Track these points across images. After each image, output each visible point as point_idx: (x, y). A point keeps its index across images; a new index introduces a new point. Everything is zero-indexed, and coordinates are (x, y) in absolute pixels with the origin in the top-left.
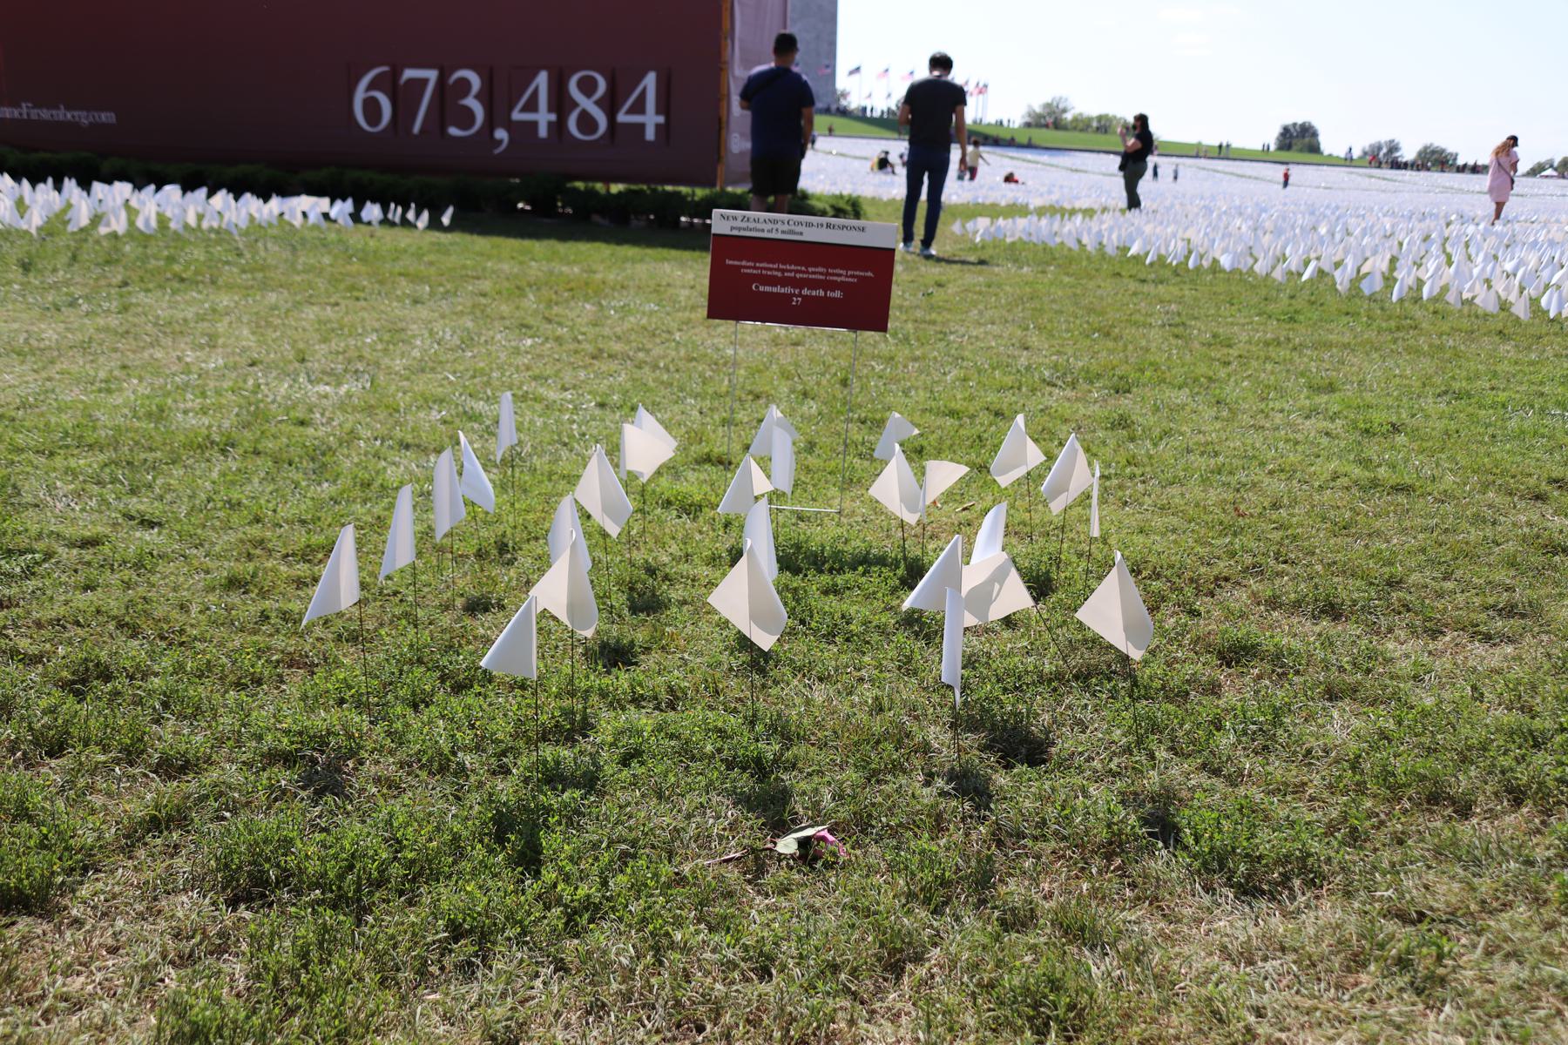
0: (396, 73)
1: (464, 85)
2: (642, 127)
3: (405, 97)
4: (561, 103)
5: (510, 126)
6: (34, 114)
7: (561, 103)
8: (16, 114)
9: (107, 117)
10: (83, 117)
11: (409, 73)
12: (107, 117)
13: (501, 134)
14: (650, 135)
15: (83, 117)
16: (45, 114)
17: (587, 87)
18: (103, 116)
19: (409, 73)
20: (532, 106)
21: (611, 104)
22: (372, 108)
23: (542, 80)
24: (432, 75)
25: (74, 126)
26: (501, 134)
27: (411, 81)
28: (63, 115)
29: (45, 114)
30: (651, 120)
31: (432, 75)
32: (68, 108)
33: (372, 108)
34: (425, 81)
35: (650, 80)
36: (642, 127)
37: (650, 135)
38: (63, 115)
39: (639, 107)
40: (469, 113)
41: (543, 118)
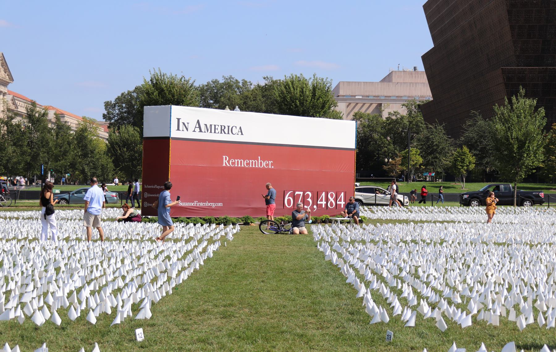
1: (308, 195)
2: (341, 204)
3: (295, 198)
4: (327, 200)
5: (317, 205)
7: (327, 200)
9: (220, 204)
10: (213, 205)
11: (297, 193)
12: (220, 204)
15: (213, 205)
16: (201, 204)
17: (332, 197)
19: (297, 193)
20: (321, 200)
21: (336, 200)
23: (324, 194)
24: (301, 193)
27: (297, 194)
28: (207, 204)
29: (201, 204)
30: (343, 203)
31: (301, 193)
33: (289, 201)
35: (342, 194)
36: (341, 204)
37: (342, 207)
38: (207, 204)
39: (340, 201)
40: (309, 202)
41: (324, 203)
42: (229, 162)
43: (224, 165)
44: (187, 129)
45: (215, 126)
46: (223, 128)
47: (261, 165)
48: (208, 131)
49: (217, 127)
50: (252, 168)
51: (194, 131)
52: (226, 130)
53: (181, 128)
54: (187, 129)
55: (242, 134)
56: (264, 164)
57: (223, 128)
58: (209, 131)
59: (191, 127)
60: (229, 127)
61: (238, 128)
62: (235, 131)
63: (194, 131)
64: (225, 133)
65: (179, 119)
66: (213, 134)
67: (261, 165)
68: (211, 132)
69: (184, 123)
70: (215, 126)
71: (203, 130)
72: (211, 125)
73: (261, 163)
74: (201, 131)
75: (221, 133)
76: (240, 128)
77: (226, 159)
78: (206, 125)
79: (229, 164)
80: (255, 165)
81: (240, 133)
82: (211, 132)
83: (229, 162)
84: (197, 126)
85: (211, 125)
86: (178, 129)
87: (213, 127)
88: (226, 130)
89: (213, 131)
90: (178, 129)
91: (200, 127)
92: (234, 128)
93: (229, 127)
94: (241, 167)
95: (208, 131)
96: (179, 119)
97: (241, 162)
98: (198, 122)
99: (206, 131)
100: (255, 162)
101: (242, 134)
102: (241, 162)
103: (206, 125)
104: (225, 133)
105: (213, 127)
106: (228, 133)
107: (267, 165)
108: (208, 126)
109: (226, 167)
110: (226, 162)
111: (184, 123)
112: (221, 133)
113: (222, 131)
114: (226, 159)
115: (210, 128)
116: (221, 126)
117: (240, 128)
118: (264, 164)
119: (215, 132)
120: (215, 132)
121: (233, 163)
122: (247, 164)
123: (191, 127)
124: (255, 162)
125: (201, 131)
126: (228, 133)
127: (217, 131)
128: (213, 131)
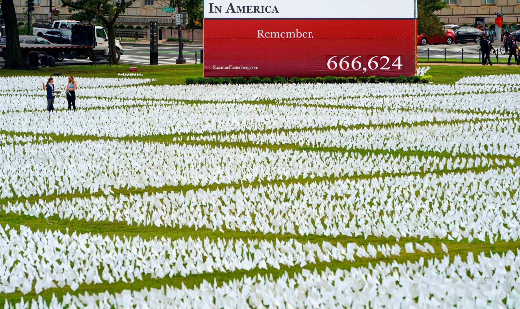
6: (233, 68)
8: (227, 68)
10: (248, 68)
13: (365, 69)
14: (399, 68)
15: (248, 68)
16: (236, 68)
18: (255, 68)
22: (332, 65)
26: (365, 69)
28: (242, 68)
29: (236, 68)
30: (399, 65)
33: (332, 65)
35: (399, 58)
37: (399, 68)
38: (242, 68)
39: (397, 63)
42: (264, 34)
43: (259, 37)
44: (220, 11)
45: (248, 7)
48: (241, 11)
50: (289, 39)
51: (227, 12)
52: (260, 10)
54: (220, 11)
55: (277, 12)
56: (303, 35)
57: (257, 8)
58: (242, 11)
59: (224, 9)
60: (263, 7)
61: (273, 8)
62: (269, 9)
63: (227, 12)
64: (259, 12)
65: (211, 5)
67: (299, 35)
68: (244, 12)
70: (248, 7)
72: (244, 7)
73: (299, 35)
74: (234, 11)
75: (255, 12)
78: (239, 7)
79: (264, 36)
82: (244, 12)
83: (264, 34)
84: (230, 8)
86: (211, 11)
88: (260, 10)
90: (211, 11)
91: (232, 9)
93: (263, 7)
94: (277, 38)
95: (241, 11)
96: (211, 5)
97: (277, 34)
98: (231, 5)
99: (239, 11)
100: (292, 34)
101: (277, 12)
102: (277, 34)
104: (259, 12)
106: (263, 12)
110: (260, 34)
111: (216, 7)
112: (255, 12)
113: (256, 10)
114: (261, 32)
115: (241, 9)
116: (255, 7)
117: (275, 7)
118: (303, 35)
119: (248, 12)
120: (248, 12)
122: (283, 36)
123: (224, 9)
124: (292, 34)
125: (234, 11)
126: (263, 12)
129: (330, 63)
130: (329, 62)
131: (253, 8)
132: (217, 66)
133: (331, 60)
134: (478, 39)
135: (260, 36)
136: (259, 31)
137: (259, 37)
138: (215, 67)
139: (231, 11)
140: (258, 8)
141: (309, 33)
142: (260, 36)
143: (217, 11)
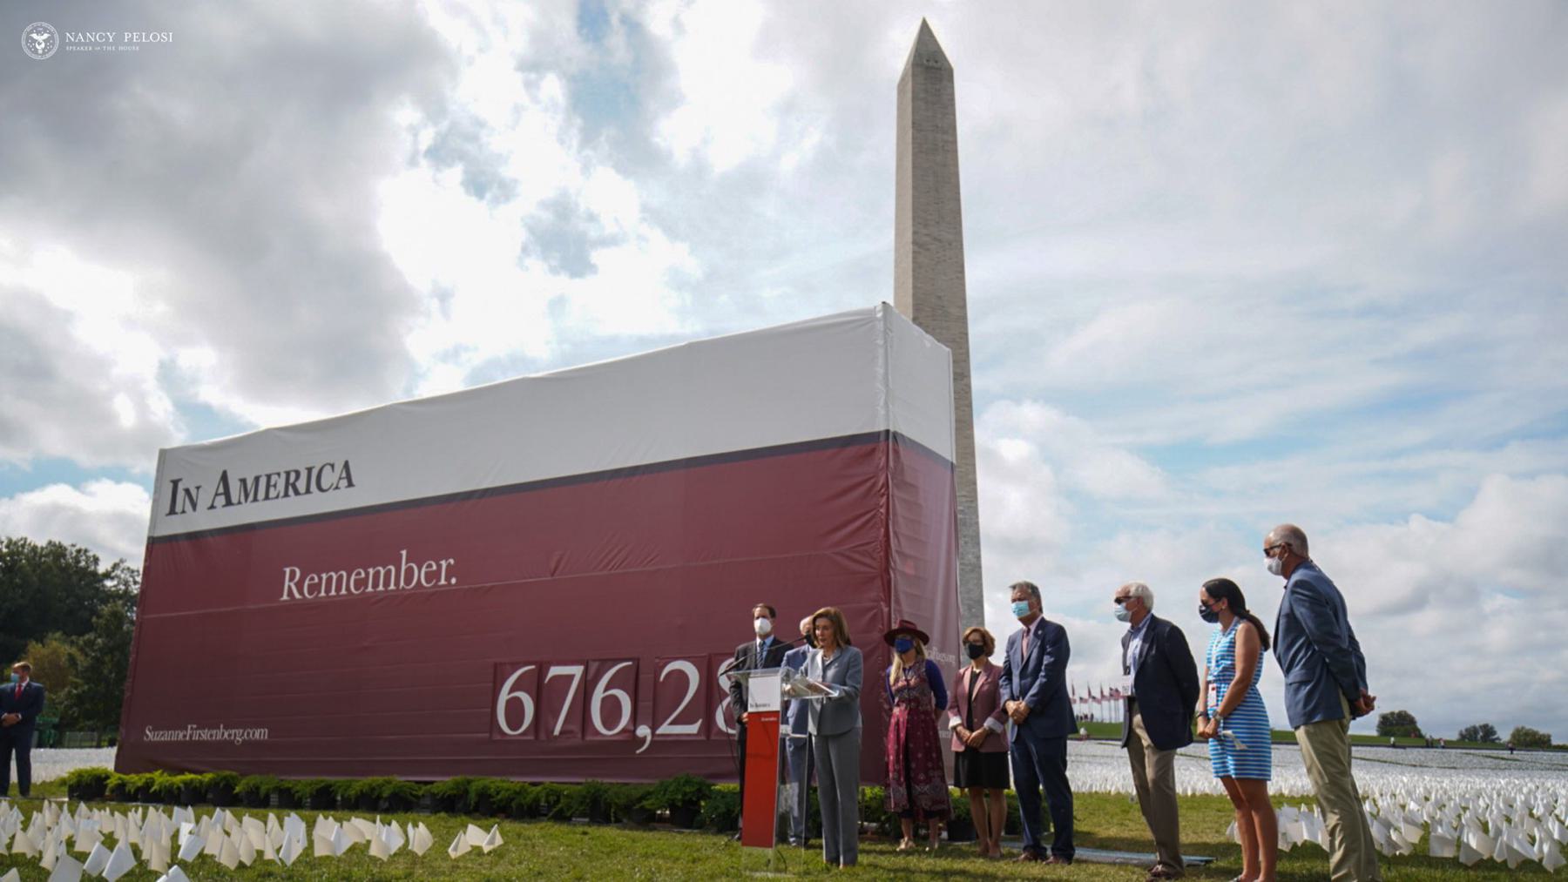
0: (542, 669)
9: (260, 734)
10: (238, 735)
11: (555, 671)
12: (260, 734)
15: (238, 735)
16: (205, 735)
19: (555, 671)
22: (515, 708)
24: (577, 671)
25: (230, 744)
28: (221, 734)
29: (205, 735)
31: (577, 671)
32: (226, 728)
33: (515, 708)
34: (571, 677)
38: (221, 734)
42: (300, 586)
43: (285, 597)
44: (194, 506)
45: (269, 477)
46: (293, 476)
47: (408, 580)
48: (247, 496)
49: (274, 479)
50: (375, 593)
51: (212, 507)
52: (301, 485)
53: (178, 508)
54: (194, 506)
55: (350, 484)
57: (293, 476)
60: (310, 470)
61: (339, 467)
63: (212, 507)
64: (297, 493)
65: (175, 483)
66: (261, 504)
68: (255, 499)
69: (187, 491)
70: (269, 477)
71: (234, 499)
72: (257, 479)
73: (409, 572)
74: (229, 503)
75: (286, 495)
76: (346, 465)
77: (293, 574)
78: (243, 481)
79: (301, 592)
80: (387, 583)
81: (344, 483)
82: (255, 499)
83: (300, 586)
84: (221, 490)
85: (257, 479)
86: (172, 512)
87: (263, 482)
88: (301, 485)
89: (261, 494)
91: (227, 493)
92: (328, 469)
93: (310, 470)
95: (247, 496)
96: (175, 483)
97: (340, 579)
98: (224, 478)
100: (388, 573)
101: (350, 484)
102: (340, 579)
103: (243, 481)
104: (297, 493)
105: (263, 482)
106: (308, 491)
107: (429, 577)
108: (250, 483)
109: (294, 606)
110: (292, 586)
111: (187, 491)
112: (286, 495)
113: (291, 487)
114: (293, 574)
116: (288, 474)
117: (346, 465)
118: (420, 575)
120: (267, 497)
121: (312, 588)
122: (358, 584)
124: (388, 573)
126: (308, 491)
127: (273, 493)
128: (261, 494)
129: (509, 702)
130: (504, 696)
131: (283, 476)
132: (155, 729)
133: (511, 691)
134: (445, 125)
135: (290, 593)
136: (288, 570)
137: (285, 597)
138: (151, 735)
139: (221, 500)
140: (298, 474)
141: (444, 563)
142: (290, 593)
143: (188, 507)
